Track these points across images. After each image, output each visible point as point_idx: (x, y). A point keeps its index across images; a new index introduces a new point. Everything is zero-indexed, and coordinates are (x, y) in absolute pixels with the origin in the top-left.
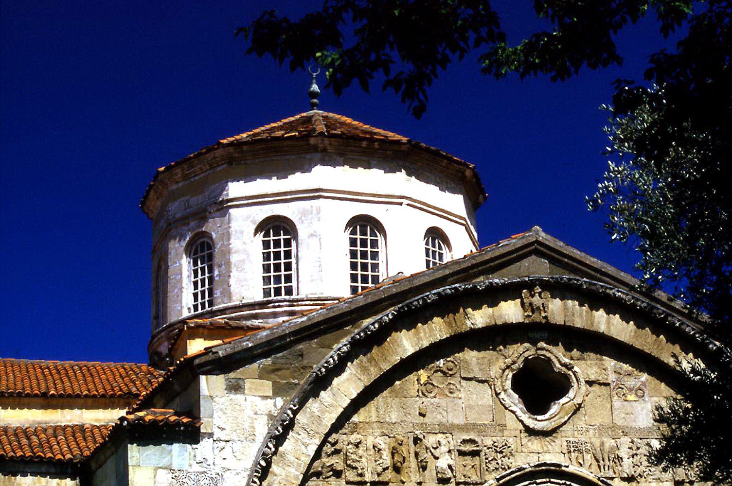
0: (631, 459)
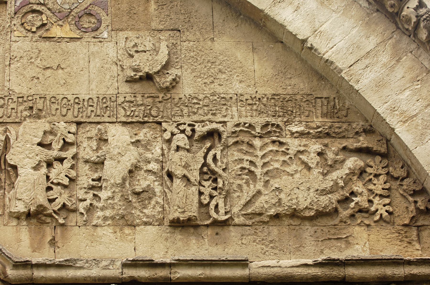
0: (44, 170)
